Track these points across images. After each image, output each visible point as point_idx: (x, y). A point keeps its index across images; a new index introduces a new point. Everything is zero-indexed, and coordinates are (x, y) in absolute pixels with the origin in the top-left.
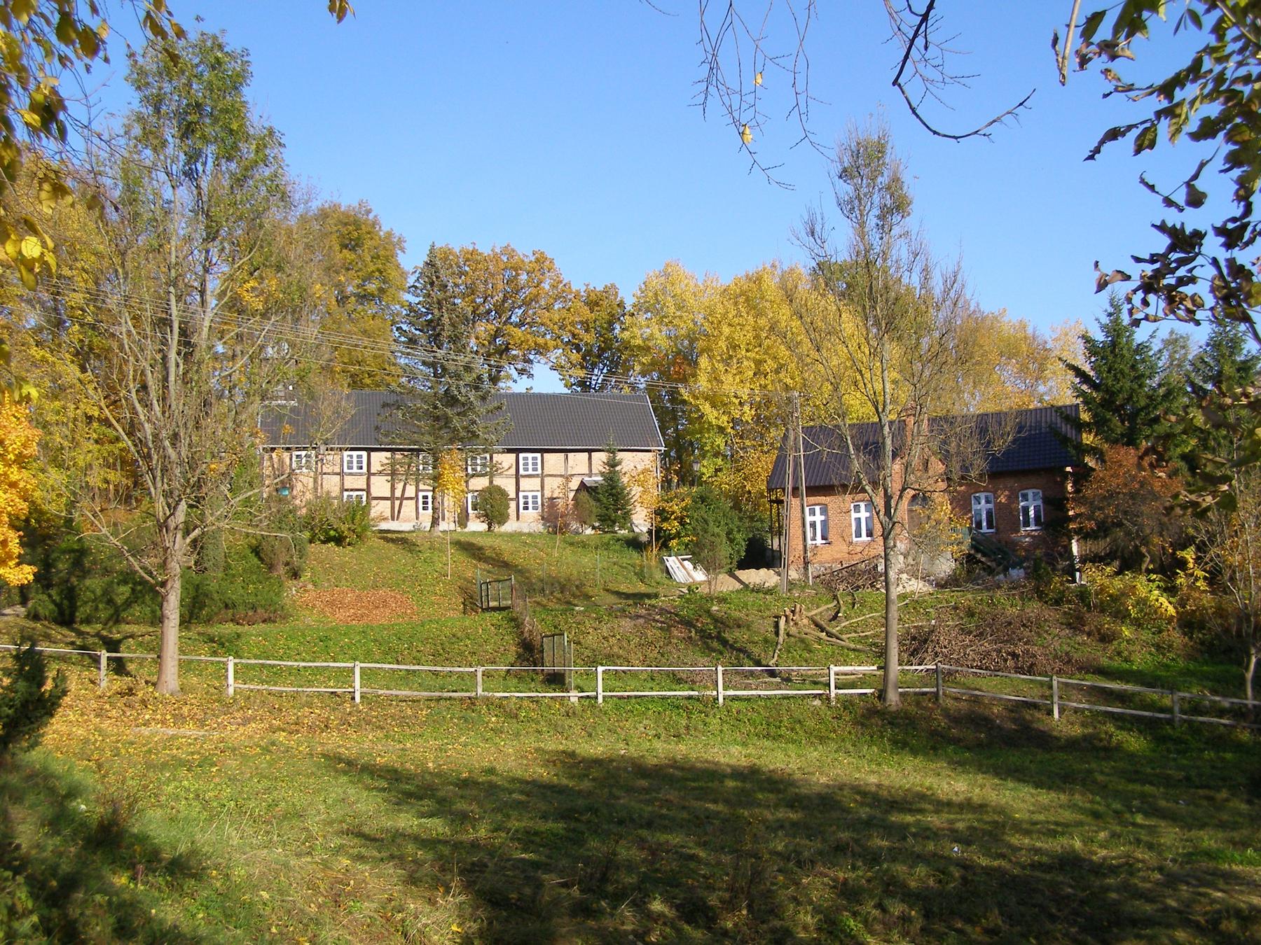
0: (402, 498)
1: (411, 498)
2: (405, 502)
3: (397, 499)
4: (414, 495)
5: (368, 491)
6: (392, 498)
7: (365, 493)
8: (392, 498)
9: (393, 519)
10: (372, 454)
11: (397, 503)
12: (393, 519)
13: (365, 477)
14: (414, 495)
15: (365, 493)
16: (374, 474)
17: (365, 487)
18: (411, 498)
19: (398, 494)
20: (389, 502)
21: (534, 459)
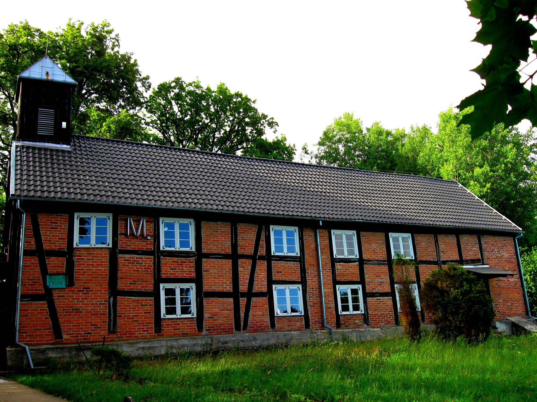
0: (250, 294)
1: (260, 294)
2: (254, 299)
3: (243, 295)
4: (265, 289)
5: (198, 281)
6: (235, 294)
7: (193, 285)
8: (235, 294)
9: (238, 328)
10: (204, 225)
11: (243, 301)
12: (238, 328)
13: (193, 259)
14: (265, 289)
15: (193, 285)
16: (207, 256)
17: (193, 275)
18: (260, 294)
19: (243, 287)
20: (231, 300)
21: (172, 244)
